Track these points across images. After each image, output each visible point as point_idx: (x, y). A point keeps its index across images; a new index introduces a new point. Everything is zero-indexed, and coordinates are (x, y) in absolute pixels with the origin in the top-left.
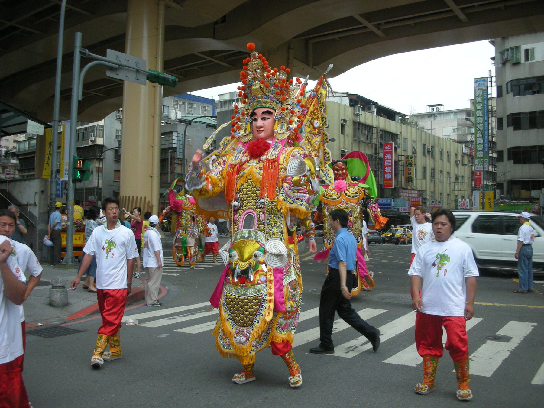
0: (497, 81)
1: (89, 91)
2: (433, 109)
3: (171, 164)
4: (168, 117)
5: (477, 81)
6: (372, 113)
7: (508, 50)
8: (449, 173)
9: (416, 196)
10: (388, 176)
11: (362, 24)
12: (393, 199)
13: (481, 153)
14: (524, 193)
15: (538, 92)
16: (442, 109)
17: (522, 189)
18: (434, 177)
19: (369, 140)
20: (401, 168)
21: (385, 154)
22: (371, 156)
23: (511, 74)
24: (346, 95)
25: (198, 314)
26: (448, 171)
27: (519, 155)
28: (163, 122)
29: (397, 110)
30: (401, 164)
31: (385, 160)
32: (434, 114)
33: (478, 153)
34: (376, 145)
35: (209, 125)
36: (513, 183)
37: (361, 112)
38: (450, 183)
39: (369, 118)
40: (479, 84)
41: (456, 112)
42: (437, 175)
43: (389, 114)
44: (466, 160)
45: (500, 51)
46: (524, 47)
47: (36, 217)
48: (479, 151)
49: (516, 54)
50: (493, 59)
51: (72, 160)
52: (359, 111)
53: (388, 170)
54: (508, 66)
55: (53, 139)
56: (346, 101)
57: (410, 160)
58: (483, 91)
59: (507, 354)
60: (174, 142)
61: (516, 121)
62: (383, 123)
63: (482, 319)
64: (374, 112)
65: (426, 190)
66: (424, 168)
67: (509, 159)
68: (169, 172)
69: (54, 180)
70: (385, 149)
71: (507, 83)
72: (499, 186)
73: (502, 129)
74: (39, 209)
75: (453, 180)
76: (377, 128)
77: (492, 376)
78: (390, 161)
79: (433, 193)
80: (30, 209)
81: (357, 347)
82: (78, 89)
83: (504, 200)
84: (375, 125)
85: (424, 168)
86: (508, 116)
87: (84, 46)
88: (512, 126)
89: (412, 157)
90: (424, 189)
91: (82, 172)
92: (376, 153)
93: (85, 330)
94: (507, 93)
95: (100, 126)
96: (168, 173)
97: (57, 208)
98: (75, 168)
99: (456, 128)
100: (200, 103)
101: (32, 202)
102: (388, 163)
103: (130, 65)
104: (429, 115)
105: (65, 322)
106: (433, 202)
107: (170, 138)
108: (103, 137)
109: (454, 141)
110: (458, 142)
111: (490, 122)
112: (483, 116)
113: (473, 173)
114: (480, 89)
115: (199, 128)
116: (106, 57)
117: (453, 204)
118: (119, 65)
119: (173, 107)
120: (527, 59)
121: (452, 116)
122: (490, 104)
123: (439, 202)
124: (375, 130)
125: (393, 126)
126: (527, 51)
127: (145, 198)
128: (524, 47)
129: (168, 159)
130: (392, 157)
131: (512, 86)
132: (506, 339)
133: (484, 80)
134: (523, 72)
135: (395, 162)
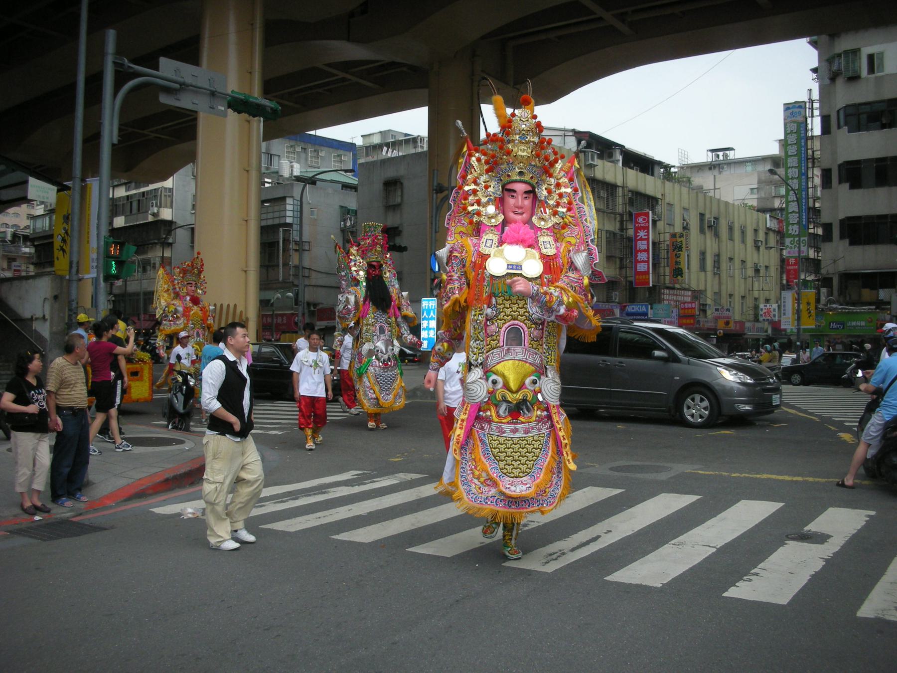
0: (821, 108)
1: (145, 132)
2: (718, 156)
3: (284, 251)
4: (277, 172)
5: (788, 107)
6: (615, 162)
7: (839, 55)
8: (743, 262)
9: (689, 299)
10: (642, 267)
11: (595, 14)
12: (651, 305)
13: (796, 227)
14: (867, 294)
15: (890, 126)
16: (731, 155)
17: (865, 287)
18: (718, 268)
19: (610, 207)
20: (664, 254)
21: (637, 230)
22: (615, 234)
23: (845, 95)
24: (571, 134)
25: (305, 498)
26: (742, 257)
27: (858, 230)
28: (266, 180)
29: (657, 158)
30: (663, 246)
31: (636, 241)
32: (719, 165)
33: (790, 228)
34: (621, 215)
35: (346, 186)
36: (848, 278)
37: (597, 161)
38: (745, 279)
39: (610, 171)
40: (792, 113)
41: (755, 161)
42: (724, 265)
43: (643, 164)
44: (773, 239)
45: (826, 57)
46: (866, 51)
47: (45, 340)
48: (793, 224)
49: (853, 62)
50: (815, 70)
51: (102, 243)
52: (593, 159)
53: (641, 256)
54: (840, 82)
55: (73, 209)
56: (571, 144)
57: (679, 240)
58: (799, 124)
59: (819, 565)
60: (289, 213)
61: (854, 174)
62: (634, 179)
63: (782, 504)
64: (618, 161)
65: (706, 290)
66: (703, 254)
67: (842, 237)
68: (281, 265)
69: (75, 278)
70: (636, 222)
71: (838, 112)
72: (826, 282)
73: (830, 187)
74: (51, 327)
75: (750, 272)
76: (623, 187)
77: (789, 603)
78: (645, 242)
79: (718, 294)
80: (37, 326)
81: (564, 554)
82: (112, 124)
83: (834, 306)
84: (619, 183)
85: (703, 254)
86: (840, 166)
87: (119, 52)
88: (847, 182)
89: (681, 236)
90: (702, 287)
91: (120, 264)
92: (622, 229)
93: (112, 527)
94: (839, 127)
95: (166, 189)
96: (278, 266)
97: (81, 324)
98: (108, 256)
99: (756, 186)
100: (331, 150)
101: (39, 314)
102: (642, 245)
103: (199, 85)
104: (710, 167)
105: (81, 514)
106: (717, 310)
107: (282, 208)
108: (172, 207)
109: (752, 208)
110: (758, 211)
111: (810, 175)
112: (799, 167)
113: (783, 261)
114: (794, 122)
115: (330, 191)
116: (157, 69)
117: (751, 312)
118: (181, 84)
119: (288, 157)
120: (871, 70)
121: (749, 168)
122: (809, 147)
123: (728, 310)
124: (620, 190)
125: (649, 184)
126: (871, 57)
127: (235, 306)
128: (866, 51)
129: (278, 242)
130: (648, 235)
131: (846, 116)
132: (820, 538)
133: (800, 107)
134: (864, 93)
135: (654, 244)
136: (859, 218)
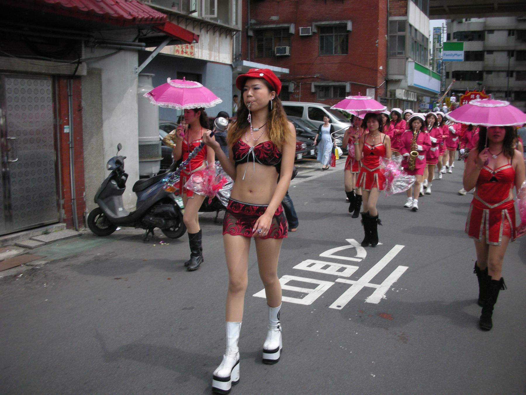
0: (447, 30)
23: (456, 28)
54: (455, 23)
67: (453, 77)
136: (459, 71)
